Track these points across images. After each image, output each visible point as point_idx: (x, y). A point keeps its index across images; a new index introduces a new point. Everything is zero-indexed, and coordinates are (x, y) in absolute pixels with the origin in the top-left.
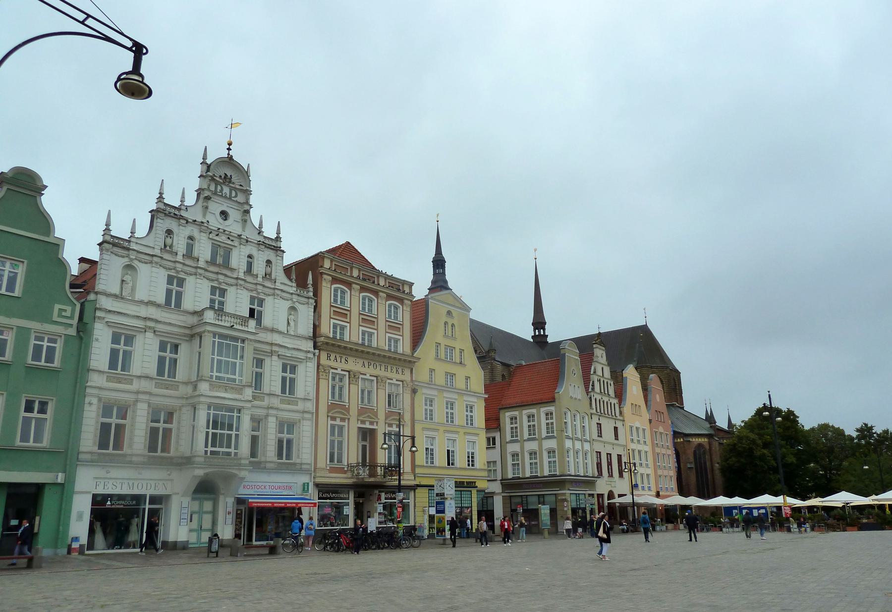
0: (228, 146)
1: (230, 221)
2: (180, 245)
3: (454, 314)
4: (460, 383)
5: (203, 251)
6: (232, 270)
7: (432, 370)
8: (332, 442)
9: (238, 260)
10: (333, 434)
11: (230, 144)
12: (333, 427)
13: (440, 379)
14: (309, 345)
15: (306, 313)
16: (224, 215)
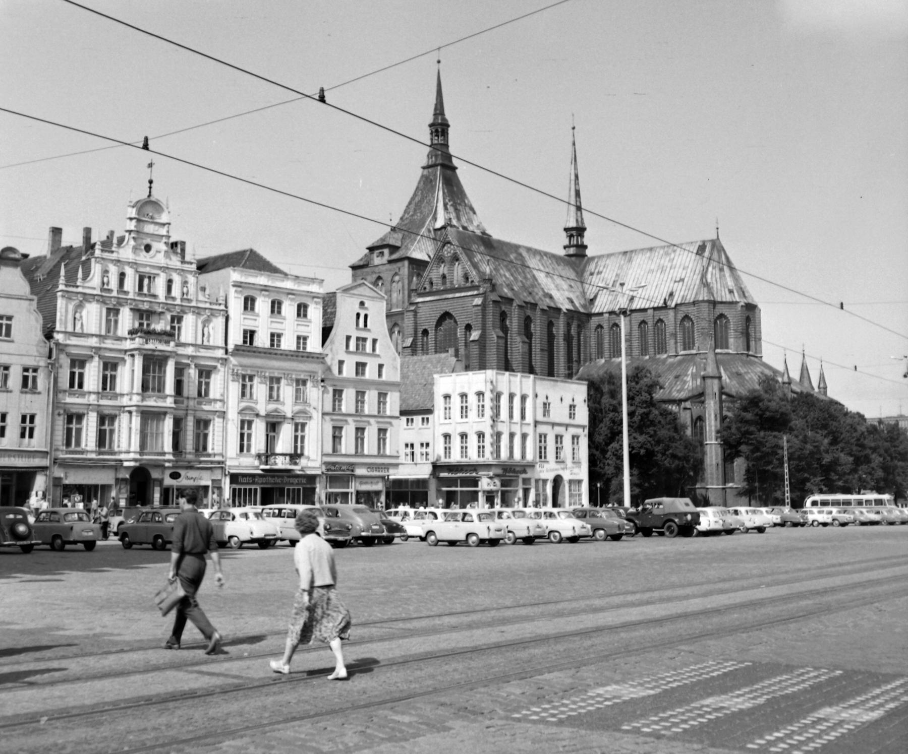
0: (149, 185)
1: (152, 252)
2: (114, 284)
3: (366, 305)
4: (370, 373)
5: (130, 284)
6: (155, 296)
7: (341, 363)
8: (242, 435)
9: (159, 287)
10: (242, 428)
12: (243, 422)
13: (349, 371)
14: (220, 353)
15: (218, 323)
16: (148, 248)
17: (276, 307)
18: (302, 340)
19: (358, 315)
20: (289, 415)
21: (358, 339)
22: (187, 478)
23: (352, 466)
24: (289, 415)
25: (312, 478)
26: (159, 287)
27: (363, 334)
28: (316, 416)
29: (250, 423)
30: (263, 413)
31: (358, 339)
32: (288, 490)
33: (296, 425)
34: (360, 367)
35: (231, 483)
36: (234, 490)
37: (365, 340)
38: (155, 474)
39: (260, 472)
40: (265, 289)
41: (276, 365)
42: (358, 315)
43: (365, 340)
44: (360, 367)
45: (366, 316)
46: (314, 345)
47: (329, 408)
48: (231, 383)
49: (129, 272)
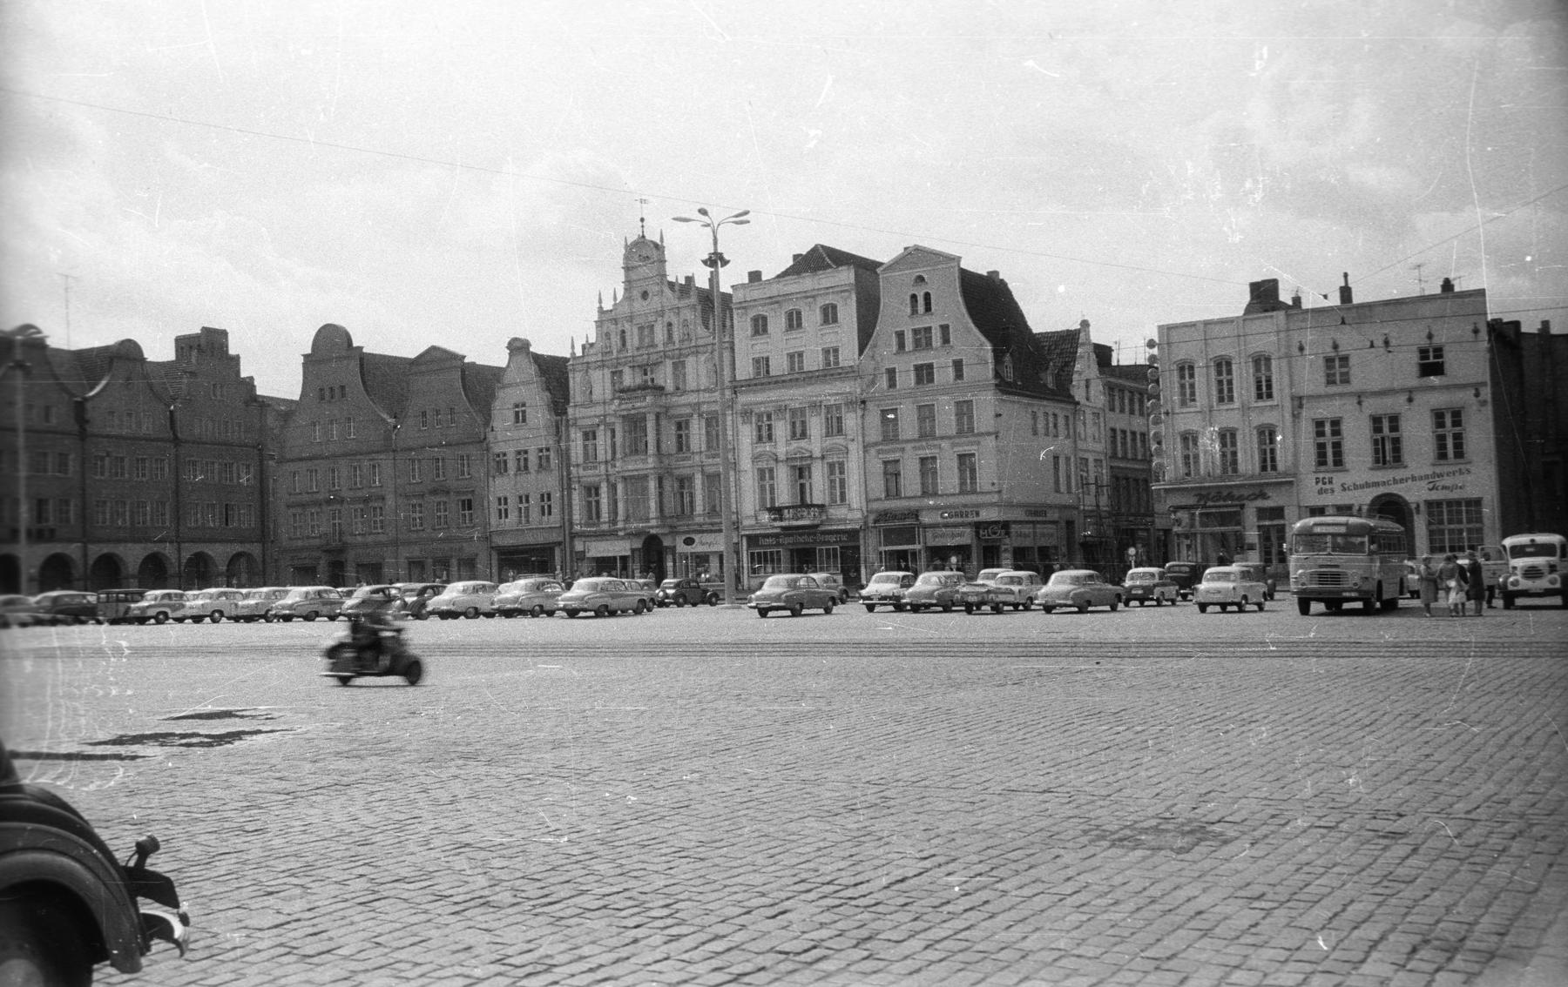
0: (640, 224)
4: (943, 375)
9: (660, 335)
11: (642, 220)
12: (761, 472)
17: (794, 321)
18: (831, 352)
19: (914, 297)
20: (817, 453)
21: (916, 332)
22: (702, 544)
23: (915, 514)
24: (817, 453)
25: (853, 534)
26: (660, 335)
27: (920, 324)
28: (855, 450)
29: (771, 471)
30: (782, 457)
31: (916, 332)
32: (821, 550)
33: (831, 466)
34: (924, 373)
35: (749, 546)
36: (752, 554)
37: (928, 330)
38: (667, 542)
39: (778, 531)
40: (810, 296)
41: (795, 396)
42: (914, 297)
43: (928, 330)
44: (924, 373)
45: (927, 296)
46: (849, 355)
47: (874, 435)
48: (740, 426)
49: (627, 326)
